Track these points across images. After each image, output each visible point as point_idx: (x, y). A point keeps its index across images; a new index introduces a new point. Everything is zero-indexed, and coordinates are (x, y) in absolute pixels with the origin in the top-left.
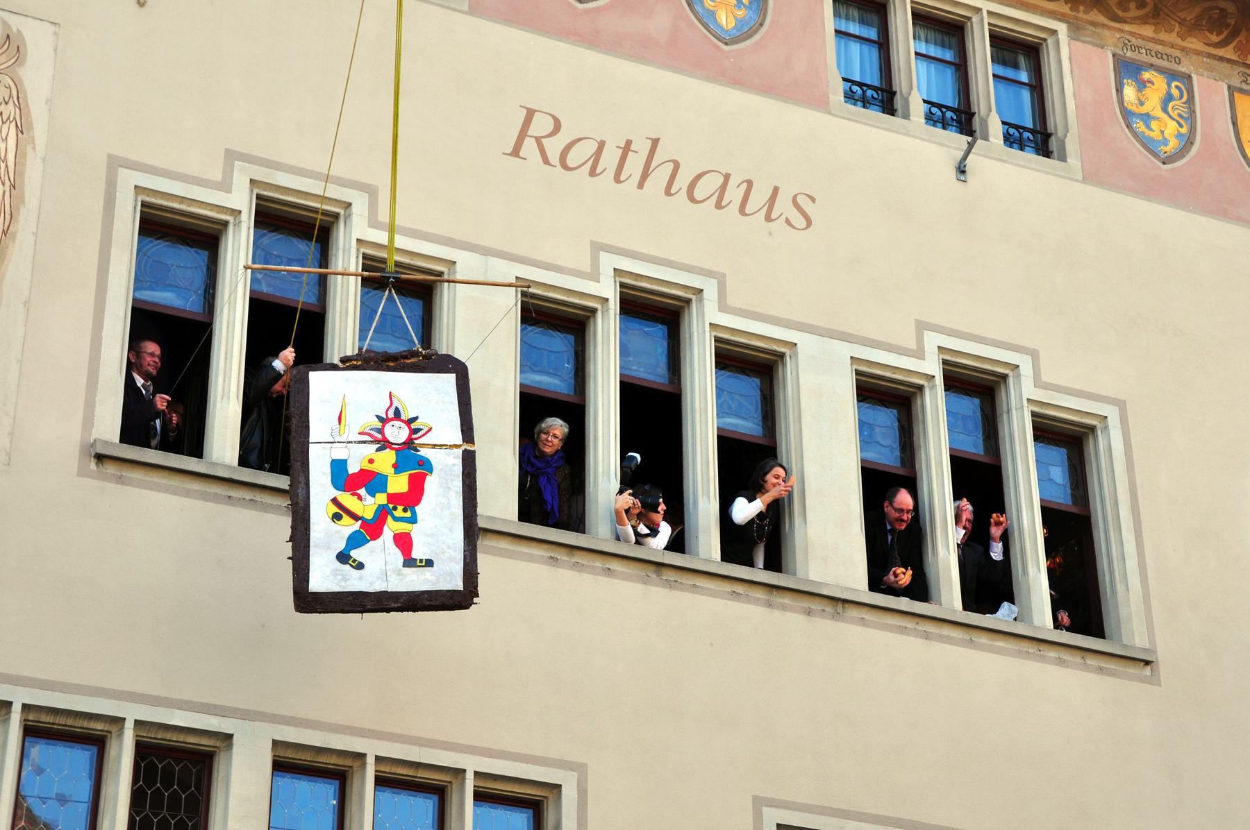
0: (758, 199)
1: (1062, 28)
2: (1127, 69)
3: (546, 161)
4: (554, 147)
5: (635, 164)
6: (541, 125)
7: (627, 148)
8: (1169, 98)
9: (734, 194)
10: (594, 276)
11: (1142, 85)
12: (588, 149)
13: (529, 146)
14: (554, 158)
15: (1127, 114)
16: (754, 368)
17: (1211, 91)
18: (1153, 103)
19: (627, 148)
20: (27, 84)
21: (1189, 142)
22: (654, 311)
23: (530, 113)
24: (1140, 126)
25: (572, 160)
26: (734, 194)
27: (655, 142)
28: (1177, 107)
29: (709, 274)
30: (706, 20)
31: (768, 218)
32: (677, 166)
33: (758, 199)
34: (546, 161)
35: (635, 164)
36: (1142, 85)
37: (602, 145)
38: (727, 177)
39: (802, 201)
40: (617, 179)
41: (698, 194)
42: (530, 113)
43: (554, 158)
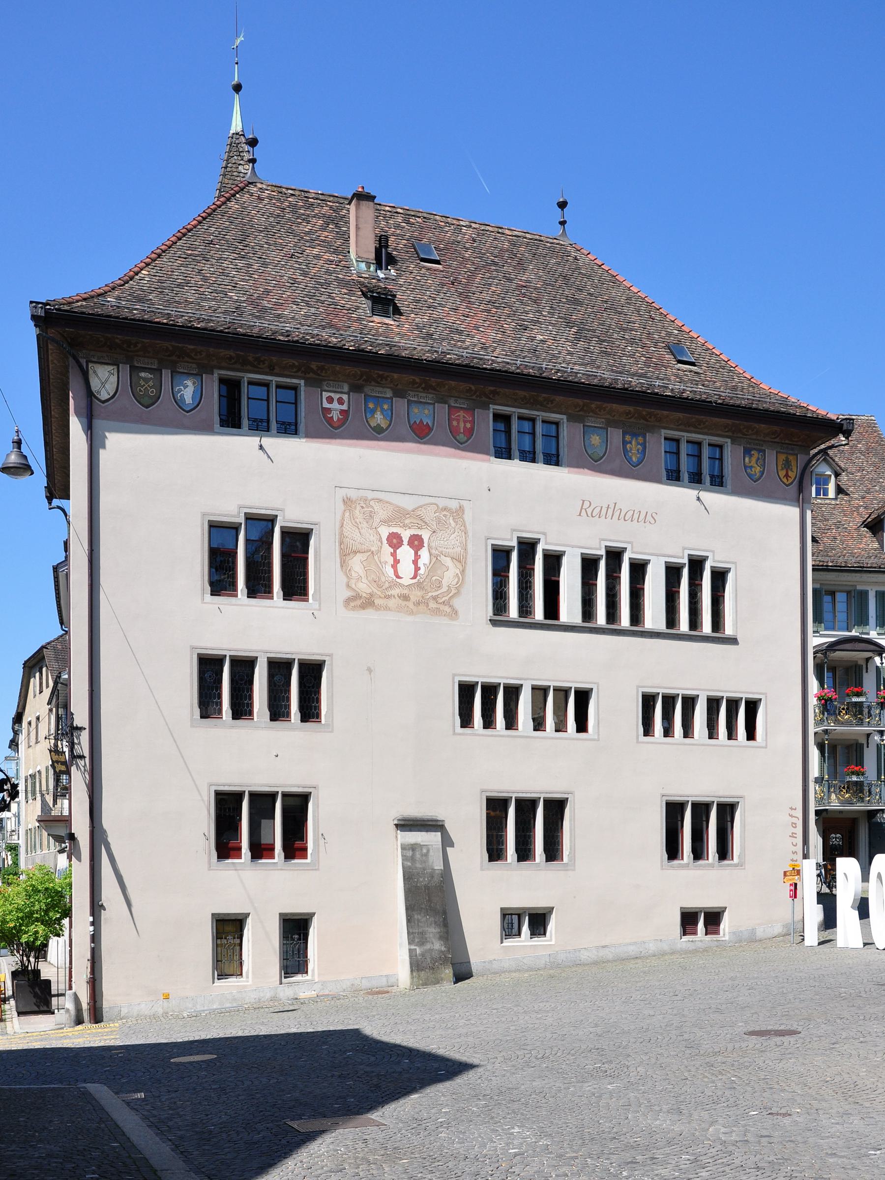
1: (729, 440)
2: (747, 452)
4: (589, 511)
5: (610, 511)
6: (586, 504)
8: (758, 459)
9: (636, 516)
11: (751, 456)
12: (598, 509)
14: (589, 514)
15: (746, 467)
17: (771, 455)
18: (754, 460)
20: (466, 519)
21: (762, 473)
24: (749, 471)
26: (636, 516)
28: (761, 462)
29: (629, 543)
30: (629, 461)
35: (610, 511)
36: (751, 456)
39: (654, 515)
43: (589, 514)
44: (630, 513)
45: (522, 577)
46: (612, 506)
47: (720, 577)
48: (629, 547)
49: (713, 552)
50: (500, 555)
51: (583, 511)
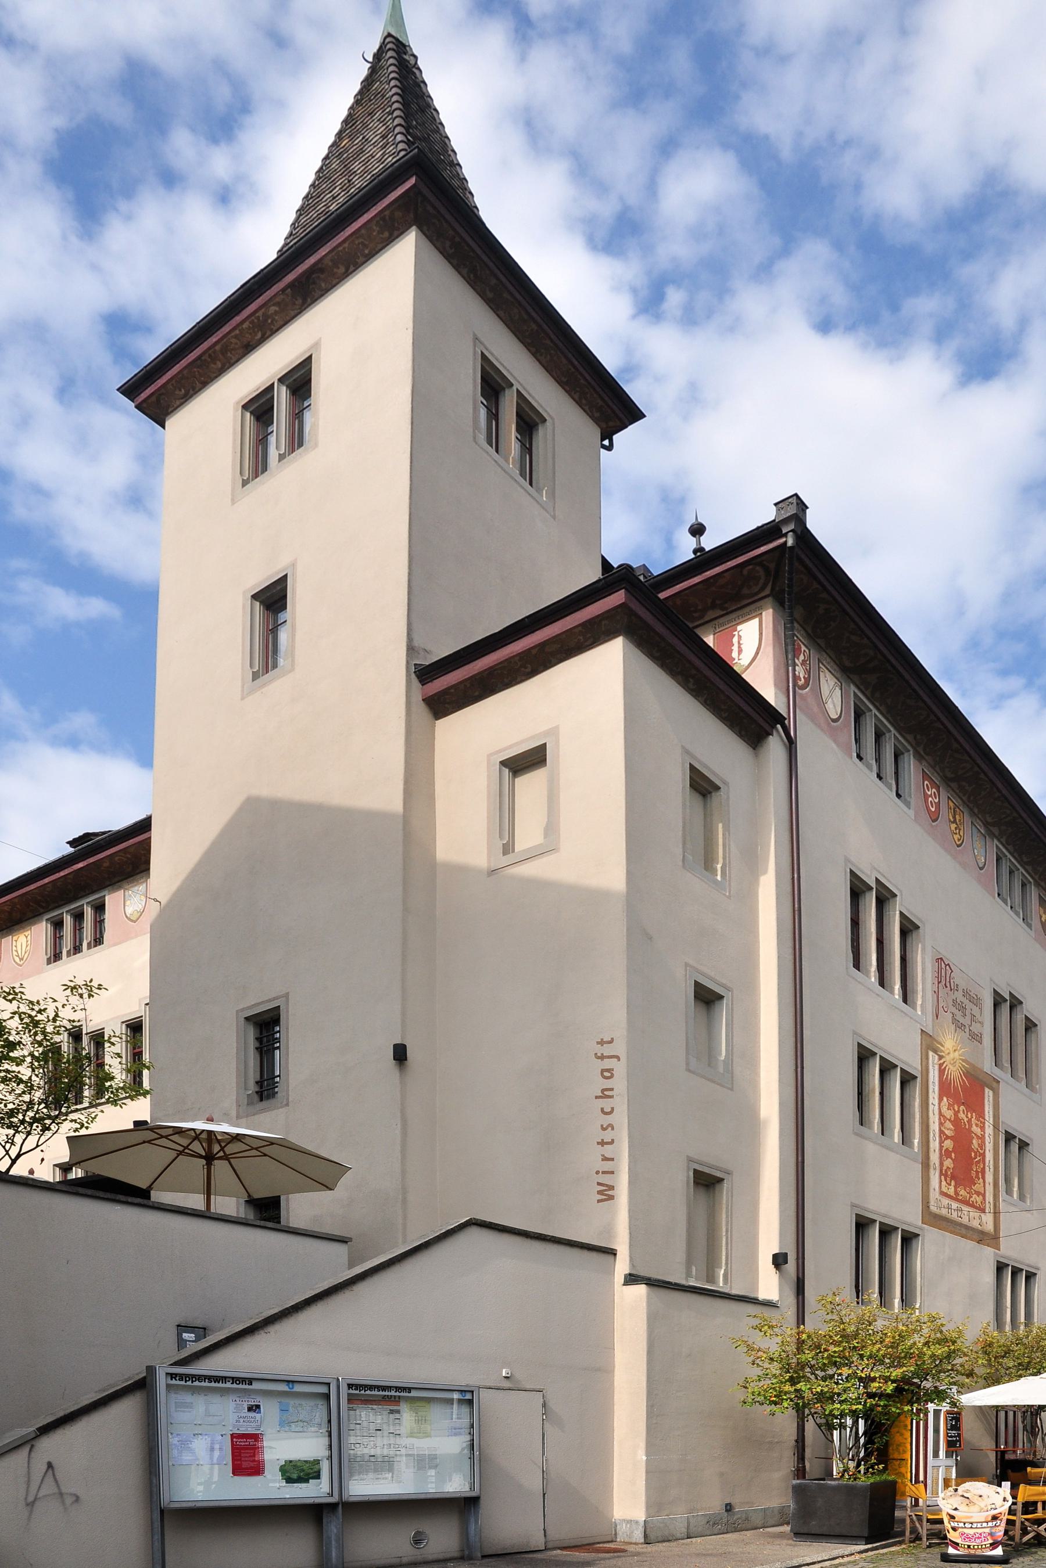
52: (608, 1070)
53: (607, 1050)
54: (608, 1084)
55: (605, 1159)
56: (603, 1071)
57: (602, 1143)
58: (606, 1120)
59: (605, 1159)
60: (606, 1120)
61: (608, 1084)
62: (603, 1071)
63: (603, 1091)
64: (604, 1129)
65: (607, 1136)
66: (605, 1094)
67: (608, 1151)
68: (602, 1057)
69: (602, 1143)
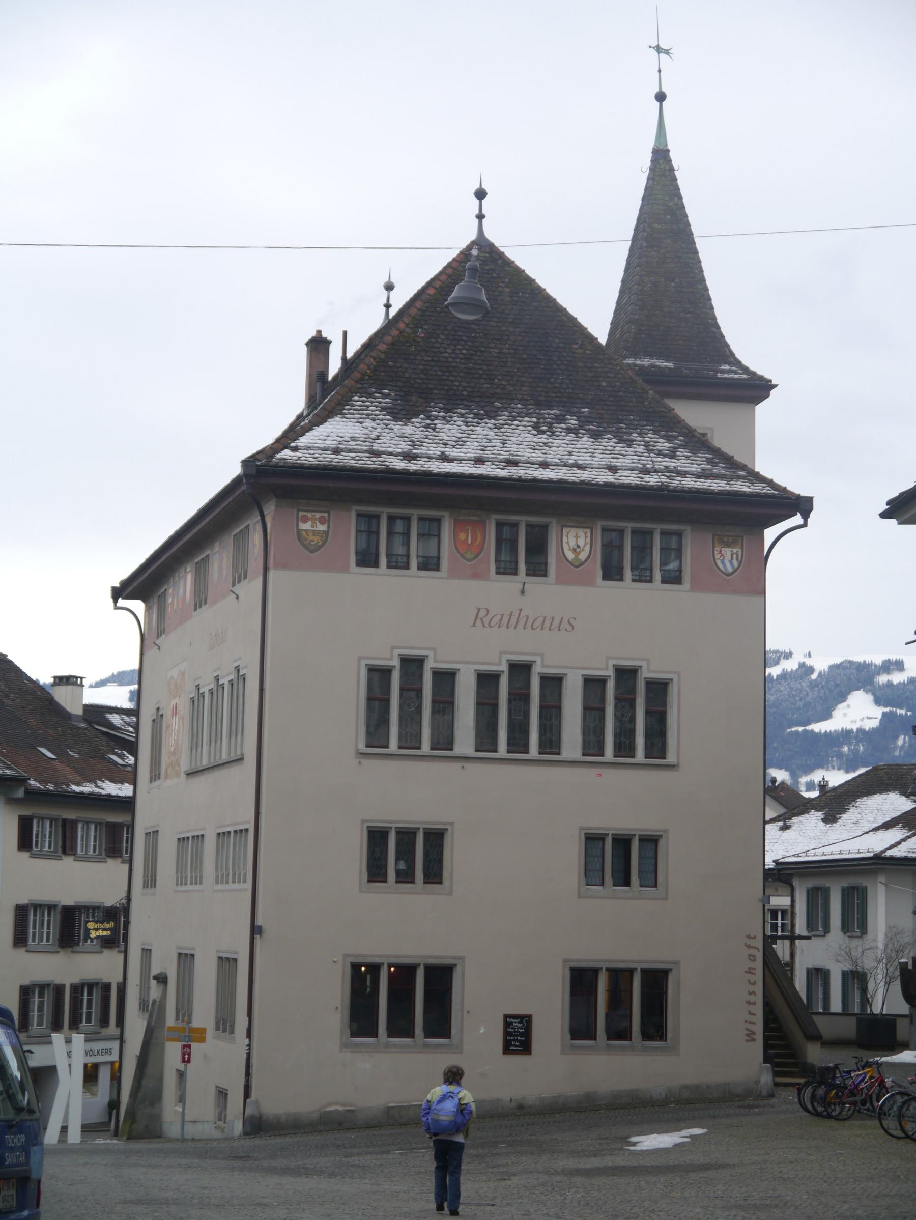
0: (556, 623)
3: (484, 626)
6: (483, 613)
7: (511, 615)
9: (547, 624)
10: (500, 664)
12: (499, 617)
13: (479, 622)
14: (487, 625)
16: (553, 684)
19: (511, 615)
22: (521, 670)
23: (479, 610)
25: (492, 624)
26: (547, 624)
27: (521, 610)
31: (559, 630)
32: (528, 617)
33: (556, 623)
34: (484, 626)
37: (502, 615)
38: (545, 618)
40: (507, 627)
41: (535, 627)
42: (479, 610)
43: (487, 625)
44: (541, 620)
45: (403, 702)
46: (516, 613)
47: (659, 690)
48: (538, 660)
49: (648, 661)
50: (378, 676)
51: (479, 621)
52: (754, 956)
53: (751, 942)
54: (752, 965)
55: (750, 1013)
56: (750, 955)
57: (749, 1003)
58: (752, 988)
59: (750, 1013)
60: (752, 988)
61: (752, 965)
62: (750, 955)
63: (750, 968)
64: (750, 994)
65: (752, 999)
66: (750, 971)
67: (752, 1008)
68: (749, 947)
69: (749, 1003)
